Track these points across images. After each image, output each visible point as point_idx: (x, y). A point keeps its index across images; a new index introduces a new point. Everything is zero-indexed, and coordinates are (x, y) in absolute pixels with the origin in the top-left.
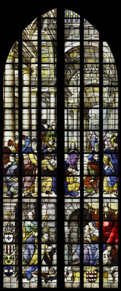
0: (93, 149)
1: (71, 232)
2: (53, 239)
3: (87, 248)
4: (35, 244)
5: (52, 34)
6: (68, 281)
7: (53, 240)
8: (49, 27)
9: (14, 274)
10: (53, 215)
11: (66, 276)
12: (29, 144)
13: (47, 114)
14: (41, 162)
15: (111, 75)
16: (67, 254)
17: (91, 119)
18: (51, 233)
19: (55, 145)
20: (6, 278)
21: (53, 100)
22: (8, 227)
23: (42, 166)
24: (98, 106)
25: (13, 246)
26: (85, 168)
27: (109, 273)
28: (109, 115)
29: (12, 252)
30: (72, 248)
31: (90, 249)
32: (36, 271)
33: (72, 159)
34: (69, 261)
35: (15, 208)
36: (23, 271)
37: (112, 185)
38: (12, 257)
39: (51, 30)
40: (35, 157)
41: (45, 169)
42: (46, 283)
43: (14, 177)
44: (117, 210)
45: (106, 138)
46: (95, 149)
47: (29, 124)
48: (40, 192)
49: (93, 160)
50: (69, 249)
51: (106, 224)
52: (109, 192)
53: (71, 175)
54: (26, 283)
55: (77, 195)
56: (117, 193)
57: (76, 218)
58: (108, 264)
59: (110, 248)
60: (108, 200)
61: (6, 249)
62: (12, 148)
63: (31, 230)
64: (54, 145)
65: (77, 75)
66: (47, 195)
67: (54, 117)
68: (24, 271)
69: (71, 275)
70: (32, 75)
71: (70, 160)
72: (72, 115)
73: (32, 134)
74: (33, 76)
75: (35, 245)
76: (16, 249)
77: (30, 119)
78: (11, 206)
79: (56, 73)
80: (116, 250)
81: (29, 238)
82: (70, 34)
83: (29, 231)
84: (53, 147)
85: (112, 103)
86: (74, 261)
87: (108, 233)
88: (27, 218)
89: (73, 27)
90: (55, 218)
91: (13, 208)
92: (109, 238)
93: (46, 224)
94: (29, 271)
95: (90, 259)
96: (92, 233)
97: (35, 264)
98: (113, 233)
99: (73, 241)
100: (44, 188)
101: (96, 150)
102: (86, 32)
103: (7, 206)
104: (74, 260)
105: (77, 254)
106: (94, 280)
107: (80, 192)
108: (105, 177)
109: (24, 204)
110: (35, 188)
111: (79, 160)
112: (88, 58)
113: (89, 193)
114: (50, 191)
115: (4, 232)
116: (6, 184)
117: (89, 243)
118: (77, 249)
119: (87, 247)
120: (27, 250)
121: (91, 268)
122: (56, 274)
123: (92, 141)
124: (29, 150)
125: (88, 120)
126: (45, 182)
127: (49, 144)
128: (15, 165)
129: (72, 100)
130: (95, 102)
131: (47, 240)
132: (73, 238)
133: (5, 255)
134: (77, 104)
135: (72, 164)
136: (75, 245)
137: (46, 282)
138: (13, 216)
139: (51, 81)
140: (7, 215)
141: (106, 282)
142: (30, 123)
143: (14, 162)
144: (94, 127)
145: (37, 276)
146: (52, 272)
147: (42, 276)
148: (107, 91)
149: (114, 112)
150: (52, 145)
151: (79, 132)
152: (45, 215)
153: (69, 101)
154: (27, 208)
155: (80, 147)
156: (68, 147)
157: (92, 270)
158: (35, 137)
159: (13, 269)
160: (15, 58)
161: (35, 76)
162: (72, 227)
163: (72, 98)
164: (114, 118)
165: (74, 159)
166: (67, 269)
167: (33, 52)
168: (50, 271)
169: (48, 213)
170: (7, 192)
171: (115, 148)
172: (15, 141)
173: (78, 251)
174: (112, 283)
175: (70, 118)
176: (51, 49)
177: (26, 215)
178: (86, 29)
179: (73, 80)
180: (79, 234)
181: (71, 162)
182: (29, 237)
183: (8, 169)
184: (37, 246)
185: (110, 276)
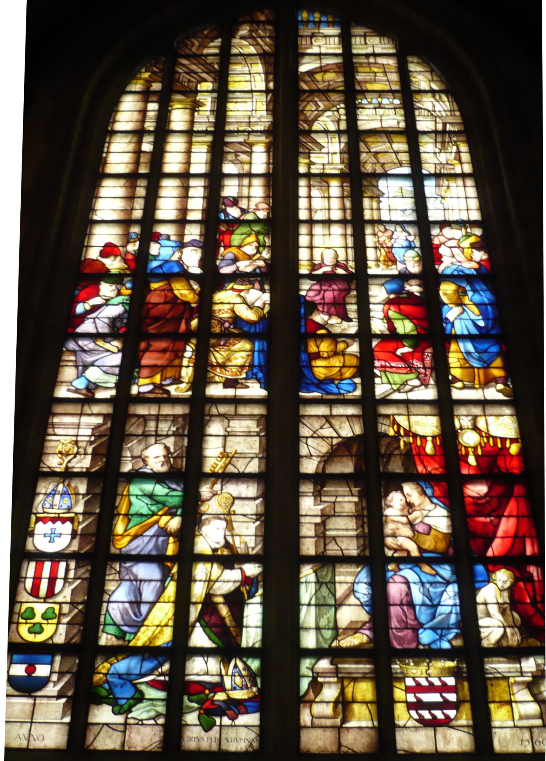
1: (329, 516)
6: (317, 722)
7: (246, 544)
9: (55, 683)
10: (251, 455)
11: (307, 698)
12: (174, 253)
16: (313, 602)
18: (241, 518)
22: (57, 497)
24: (406, 170)
29: (57, 589)
30: (334, 575)
31: (415, 583)
32: (161, 674)
34: (323, 631)
35: (96, 431)
36: (101, 673)
37: (484, 362)
38: (57, 612)
42: (207, 728)
43: (108, 339)
49: (402, 294)
50: (319, 583)
52: (474, 381)
54: (104, 724)
56: (506, 385)
58: (504, 644)
59: (505, 578)
61: (34, 578)
63: (154, 508)
64: (261, 253)
65: (338, 111)
66: (230, 392)
68: (104, 671)
75: (167, 566)
76: (78, 578)
81: (141, 535)
83: (145, 511)
84: (258, 259)
86: (344, 633)
87: (491, 521)
88: (142, 464)
90: (259, 466)
91: (89, 432)
92: (494, 536)
94: (128, 674)
95: (421, 625)
96: (421, 522)
100: (218, 370)
101: (414, 268)
104: (346, 629)
105: (358, 603)
106: (447, 716)
107: (362, 384)
109: (134, 420)
113: (395, 384)
115: (35, 514)
118: (358, 583)
119: (402, 573)
120: (125, 587)
121: (424, 661)
122: (254, 689)
124: (171, 267)
131: (218, 543)
132: (338, 540)
134: (341, 166)
135: (327, 304)
137: (207, 728)
138: (84, 458)
140: (60, 453)
141: (505, 724)
143: (112, 298)
145: (161, 695)
146: (238, 680)
147: (186, 698)
150: (254, 255)
153: (312, 159)
154: (144, 431)
156: (311, 259)
159: (51, 663)
162: (333, 499)
165: (334, 290)
166: (312, 669)
167: (207, 73)
168: (227, 675)
169: (228, 450)
170: (71, 382)
171: (478, 263)
174: (535, 731)
177: (136, 453)
181: (323, 298)
182: (140, 532)
183: (89, 316)
185: (524, 695)
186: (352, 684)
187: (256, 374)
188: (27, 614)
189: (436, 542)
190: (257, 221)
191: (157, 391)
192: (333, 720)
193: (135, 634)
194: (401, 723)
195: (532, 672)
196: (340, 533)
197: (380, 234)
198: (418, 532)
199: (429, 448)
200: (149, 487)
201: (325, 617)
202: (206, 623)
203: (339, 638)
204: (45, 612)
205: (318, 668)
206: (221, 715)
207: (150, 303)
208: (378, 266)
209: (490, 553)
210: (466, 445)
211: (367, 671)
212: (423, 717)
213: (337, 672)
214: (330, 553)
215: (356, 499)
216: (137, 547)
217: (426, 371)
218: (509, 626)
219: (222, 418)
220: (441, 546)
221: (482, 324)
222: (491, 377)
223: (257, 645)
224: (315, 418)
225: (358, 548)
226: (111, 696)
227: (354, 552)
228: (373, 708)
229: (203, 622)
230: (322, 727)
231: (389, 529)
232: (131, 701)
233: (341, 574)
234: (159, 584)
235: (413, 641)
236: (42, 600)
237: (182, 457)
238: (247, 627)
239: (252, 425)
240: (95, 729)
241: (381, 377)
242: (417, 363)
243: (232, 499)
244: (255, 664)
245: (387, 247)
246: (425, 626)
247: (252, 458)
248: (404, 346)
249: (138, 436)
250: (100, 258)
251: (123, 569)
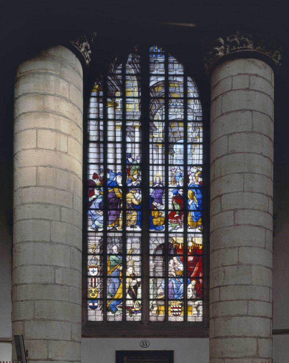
0: (178, 184)
1: (156, 266)
2: (138, 272)
3: (172, 282)
4: (120, 278)
5: (137, 68)
6: (153, 315)
7: (137, 273)
8: (133, 61)
9: (99, 307)
12: (114, 178)
13: (132, 148)
14: (126, 196)
15: (195, 110)
16: (152, 288)
17: (176, 154)
18: (136, 267)
19: (140, 179)
20: (91, 311)
21: (137, 134)
22: (93, 261)
23: (127, 200)
24: (182, 141)
26: (170, 202)
27: (193, 307)
28: (193, 150)
32: (121, 305)
37: (197, 220)
38: (97, 291)
39: (135, 64)
40: (120, 191)
41: (130, 203)
42: (131, 317)
43: (99, 211)
45: (190, 173)
46: (180, 184)
47: (114, 157)
48: (124, 226)
50: (153, 283)
51: (191, 259)
53: (155, 209)
56: (201, 227)
57: (160, 252)
58: (192, 298)
60: (193, 235)
61: (91, 282)
62: (97, 182)
63: (116, 264)
64: (139, 178)
65: (162, 110)
66: (132, 229)
67: (139, 152)
68: (109, 304)
69: (155, 309)
70: (116, 108)
71: (155, 194)
72: (157, 149)
73: (116, 167)
74: (118, 110)
77: (115, 153)
78: (95, 240)
79: (140, 107)
81: (114, 271)
82: (155, 68)
83: (114, 265)
84: (138, 181)
85: (196, 138)
88: (112, 251)
89: (158, 62)
91: (98, 242)
92: (193, 272)
95: (175, 294)
98: (198, 267)
99: (157, 274)
101: (181, 185)
102: (170, 66)
107: (165, 227)
108: (189, 212)
109: (109, 238)
110: (120, 222)
111: (164, 194)
112: (172, 93)
116: (91, 217)
117: (173, 277)
119: (172, 281)
122: (140, 308)
123: (177, 175)
124: (114, 184)
125: (172, 154)
126: (130, 216)
128: (100, 198)
129: (157, 134)
130: (180, 137)
131: (131, 273)
132: (158, 272)
136: (160, 279)
138: (98, 250)
139: (136, 115)
140: (92, 248)
141: (190, 316)
142: (115, 157)
144: (178, 163)
145: (121, 309)
146: (137, 306)
148: (192, 126)
149: (198, 147)
150: (137, 179)
151: (164, 167)
153: (154, 135)
154: (112, 242)
155: (165, 181)
156: (153, 181)
158: (120, 171)
159: (98, 303)
160: (100, 91)
161: (120, 110)
162: (157, 261)
163: (157, 132)
164: (198, 153)
165: (159, 193)
166: (152, 303)
167: (118, 86)
171: (199, 183)
173: (163, 285)
174: (196, 317)
175: (154, 152)
176: (136, 83)
178: (171, 63)
179: (158, 114)
181: (156, 196)
184: (122, 280)
185: (195, 309)
188: (91, 291)
190: (137, 164)
193: (115, 296)
194: (170, 315)
196: (159, 271)
199: (180, 247)
200: (114, 257)
206: (134, 313)
207: (109, 198)
208: (171, 184)
209: (191, 276)
213: (157, 304)
214: (156, 276)
215: (162, 262)
220: (181, 274)
221: (197, 206)
223: (140, 298)
224: (153, 238)
227: (161, 276)
228: (164, 312)
231: (170, 269)
233: (159, 281)
240: (109, 317)
244: (140, 302)
248: (176, 214)
249: (110, 243)
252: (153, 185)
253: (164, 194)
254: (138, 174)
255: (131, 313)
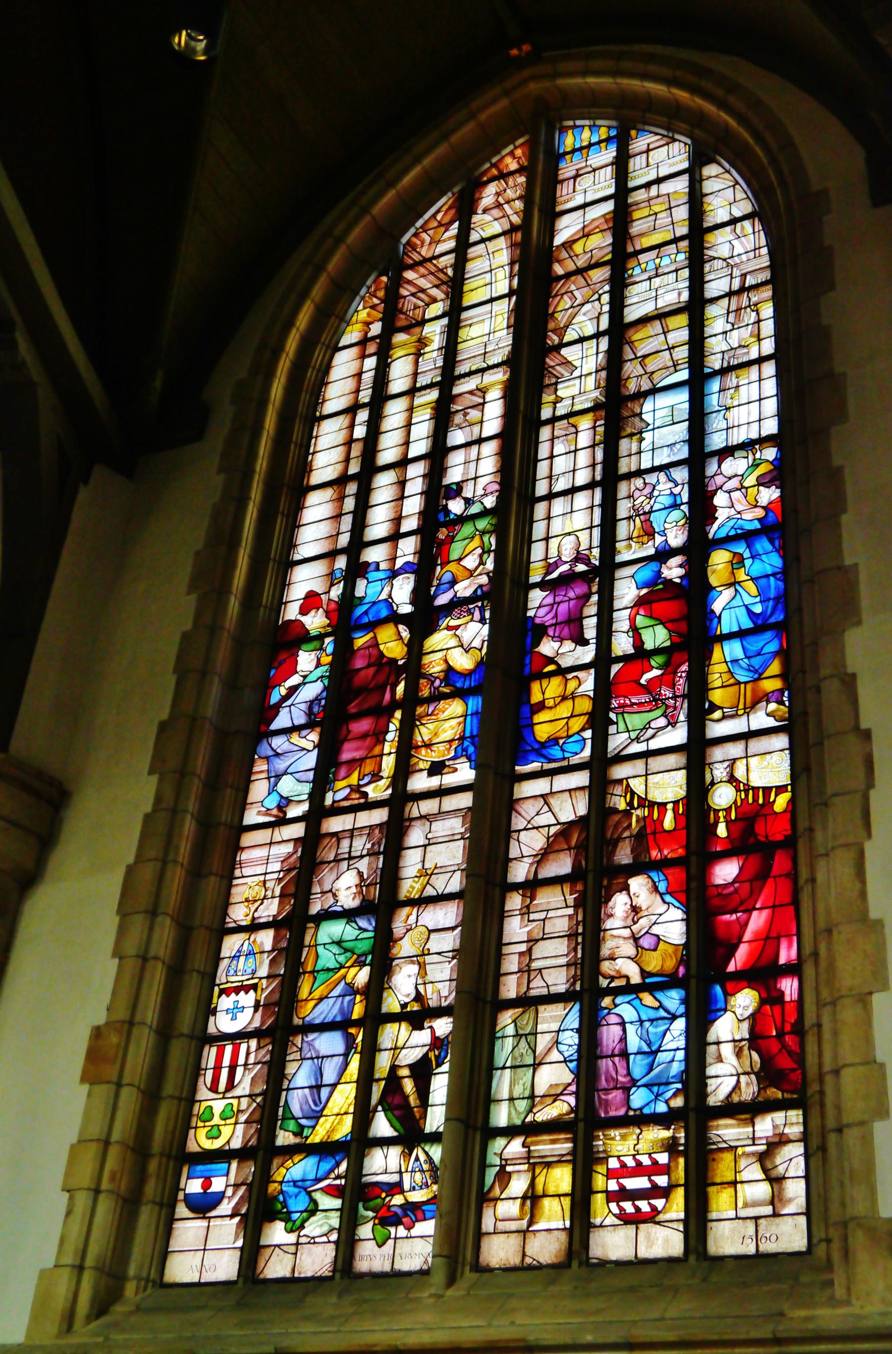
0: (659, 539)
1: (537, 941)
6: (501, 1226)
10: (453, 868)
11: (492, 1195)
18: (436, 958)
22: (242, 959)
25: (248, 1047)
26: (621, 621)
27: (744, 1154)
31: (631, 1023)
32: (338, 1177)
33: (559, 603)
34: (516, 1102)
35: (285, 864)
36: (276, 1182)
37: (756, 671)
38: (235, 1109)
40: (399, 633)
44: (787, 785)
48: (404, 770)
50: (518, 1036)
52: (737, 707)
54: (276, 1246)
55: (578, 751)
57: (562, 865)
58: (736, 1099)
59: (747, 1002)
60: (735, 750)
62: (315, 622)
63: (342, 959)
66: (434, 782)
68: (280, 1179)
69: (518, 1185)
79: (512, 321)
80: (787, 1007)
81: (326, 997)
83: (332, 964)
84: (480, 574)
86: (541, 1103)
87: (738, 918)
88: (332, 901)
92: (740, 941)
93: (413, 918)
94: (303, 1180)
95: (634, 1082)
96: (647, 932)
97: (338, 1136)
98: (765, 913)
103: (253, 862)
106: (654, 1208)
107: (592, 738)
109: (326, 841)
111: (595, 598)
114: (449, 760)
115: (219, 985)
117: (629, 989)
118: (564, 1030)
119: (616, 1010)
121: (633, 1133)
124: (378, 611)
127: (465, 567)
129: (574, 385)
133: (201, 1101)
134: (596, 394)
138: (272, 903)
140: (247, 900)
143: (311, 672)
145: (337, 1203)
146: (418, 1176)
147: (361, 1205)
152: (416, 877)
154: (337, 855)
155: (602, 546)
157: (643, 1147)
160: (372, 323)
161: (435, 354)
165: (570, 599)
172: (329, 592)
173: (570, 1039)
176: (503, 257)
177: (327, 888)
179: (584, 318)
180: (577, 944)
181: (556, 616)
182: (325, 994)
184: (360, 1039)
185: (754, 1172)
186: (545, 1171)
187: (465, 750)
188: (206, 1116)
189: (663, 960)
190: (485, 513)
191: (354, 796)
192: (518, 1222)
193: (314, 1127)
194: (598, 1221)
195: (767, 1138)
197: (637, 494)
198: (643, 948)
199: (669, 822)
201: (521, 1082)
202: (389, 1105)
203: (535, 1110)
204: (223, 1111)
205: (508, 1153)
206: (397, 1222)
209: (731, 968)
210: (717, 808)
211: (564, 1153)
212: (625, 1210)
214: (533, 993)
215: (571, 911)
216: (321, 1013)
217: (676, 701)
218: (745, 1073)
219: (424, 821)
222: (761, 695)
225: (568, 981)
226: (285, 1210)
227: (562, 989)
229: (385, 1104)
230: (505, 1232)
232: (305, 1214)
233: (546, 1021)
234: (341, 1058)
235: (623, 1106)
236: (221, 1096)
237: (376, 884)
238: (432, 1106)
239: (456, 825)
241: (617, 723)
242: (666, 692)
243: (427, 933)
245: (645, 513)
246: (639, 1084)
247: (454, 871)
248: (651, 668)
250: (300, 617)
251: (305, 1045)
252: (548, 573)
253: (595, 598)
254: (483, 549)
255: (387, 1219)
